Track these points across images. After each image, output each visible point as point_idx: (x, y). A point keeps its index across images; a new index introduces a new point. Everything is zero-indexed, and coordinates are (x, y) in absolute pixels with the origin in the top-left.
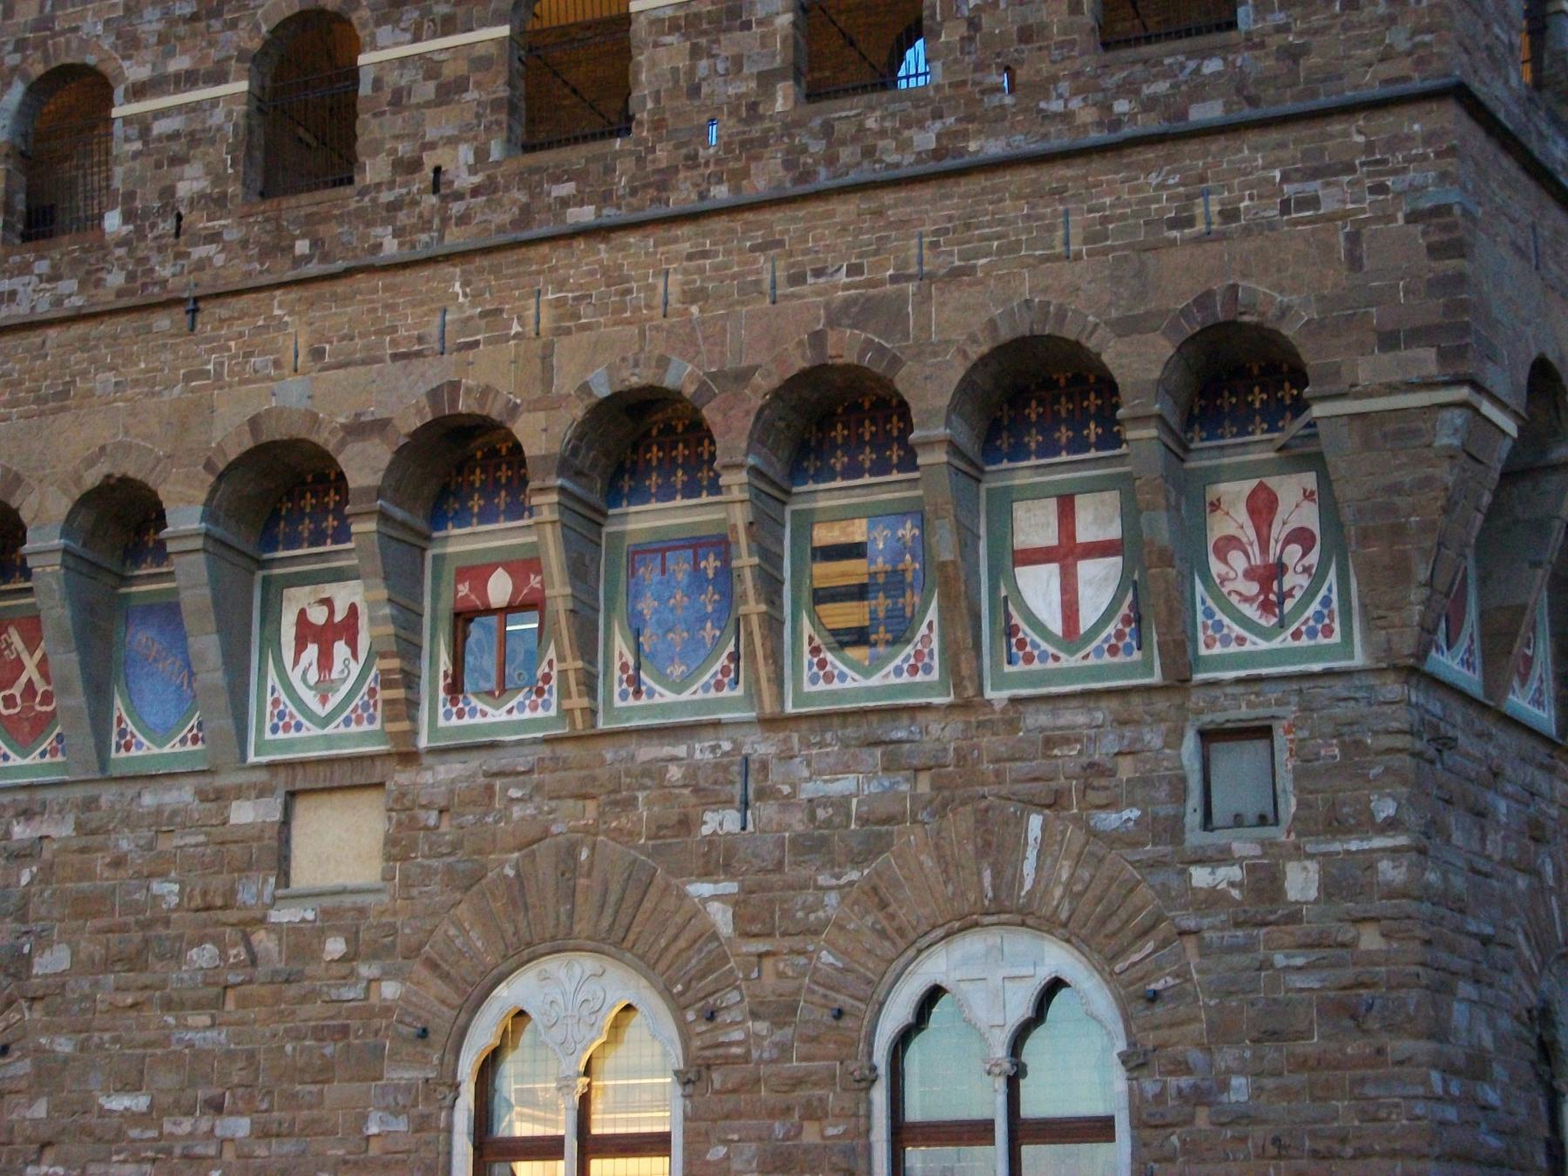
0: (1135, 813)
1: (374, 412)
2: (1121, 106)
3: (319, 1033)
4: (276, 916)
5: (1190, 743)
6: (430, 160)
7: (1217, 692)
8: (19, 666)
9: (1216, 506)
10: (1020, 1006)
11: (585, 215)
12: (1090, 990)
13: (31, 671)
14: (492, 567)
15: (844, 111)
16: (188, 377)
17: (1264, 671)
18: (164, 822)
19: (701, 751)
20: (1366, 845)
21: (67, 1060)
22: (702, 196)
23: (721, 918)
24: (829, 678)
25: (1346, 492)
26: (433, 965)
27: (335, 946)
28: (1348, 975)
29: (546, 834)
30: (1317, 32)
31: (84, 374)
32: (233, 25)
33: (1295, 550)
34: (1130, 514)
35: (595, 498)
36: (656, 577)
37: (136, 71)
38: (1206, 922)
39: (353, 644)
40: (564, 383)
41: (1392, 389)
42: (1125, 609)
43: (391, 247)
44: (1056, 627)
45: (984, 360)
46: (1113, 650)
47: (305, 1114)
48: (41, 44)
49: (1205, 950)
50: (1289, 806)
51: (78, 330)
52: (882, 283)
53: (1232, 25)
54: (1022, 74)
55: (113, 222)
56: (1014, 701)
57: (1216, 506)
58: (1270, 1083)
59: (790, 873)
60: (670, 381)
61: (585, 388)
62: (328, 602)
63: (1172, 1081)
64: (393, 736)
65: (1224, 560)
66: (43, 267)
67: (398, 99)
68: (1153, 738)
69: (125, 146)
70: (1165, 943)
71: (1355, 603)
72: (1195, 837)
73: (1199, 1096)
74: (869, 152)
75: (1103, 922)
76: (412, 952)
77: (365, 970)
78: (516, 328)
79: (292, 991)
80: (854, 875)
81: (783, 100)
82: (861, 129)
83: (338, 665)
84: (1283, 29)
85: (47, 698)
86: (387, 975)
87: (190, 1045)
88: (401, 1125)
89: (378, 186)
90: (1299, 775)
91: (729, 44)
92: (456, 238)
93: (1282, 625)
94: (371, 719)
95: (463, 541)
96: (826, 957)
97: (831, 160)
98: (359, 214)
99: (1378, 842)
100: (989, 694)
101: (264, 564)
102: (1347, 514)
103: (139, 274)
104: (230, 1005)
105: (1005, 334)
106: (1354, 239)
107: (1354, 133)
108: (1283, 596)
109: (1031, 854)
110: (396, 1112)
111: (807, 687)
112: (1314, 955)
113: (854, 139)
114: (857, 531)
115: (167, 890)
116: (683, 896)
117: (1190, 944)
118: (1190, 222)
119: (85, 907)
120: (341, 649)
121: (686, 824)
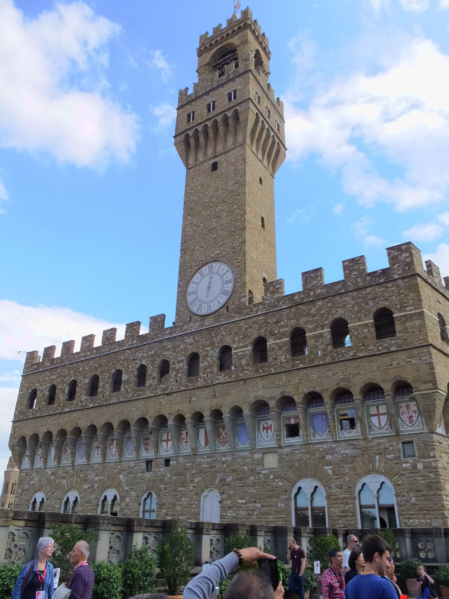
0: (393, 455)
1: (272, 396)
2: (380, 348)
3: (270, 491)
4: (262, 472)
5: (400, 445)
6: (278, 358)
7: (403, 436)
8: (222, 433)
9: (401, 407)
10: (379, 487)
11: (301, 366)
12: (389, 484)
13: (224, 434)
14: (291, 418)
15: (339, 349)
16: (245, 391)
17: (411, 433)
18: (245, 458)
19: (325, 446)
20: (429, 460)
21: (233, 495)
22: (319, 363)
23: (330, 472)
24: (344, 434)
25: (420, 405)
26: (286, 480)
27: (272, 477)
28: (429, 481)
29: (302, 459)
30: (409, 336)
31: (230, 391)
32: (248, 339)
33: (414, 414)
34: (387, 408)
35: (306, 408)
36: (316, 419)
37: (235, 346)
38: (406, 473)
39: (271, 430)
40: (300, 391)
41: (425, 390)
42: (388, 423)
43: (273, 371)
44: (378, 426)
45: (363, 386)
46: (387, 430)
47: (269, 503)
48: (221, 342)
49: (406, 477)
50: (417, 454)
51: (229, 384)
52: (346, 375)
53: (396, 336)
54: (365, 344)
55: (233, 368)
56: (373, 438)
57: (401, 407)
58: (418, 498)
59: (340, 465)
60: (316, 390)
61: (304, 391)
62: (267, 423)
63: (403, 498)
64: (278, 444)
65: (403, 415)
66: (223, 375)
67: (273, 349)
68: (395, 444)
69: (234, 357)
70: (399, 476)
71: (424, 422)
72: (403, 459)
73: (407, 501)
74: (343, 356)
75: (390, 473)
76: (283, 478)
77: (276, 480)
78: (293, 383)
79: (265, 484)
80: (350, 465)
81: (330, 348)
82: (342, 352)
83: (269, 433)
84: (403, 336)
85: (226, 438)
86: (280, 481)
87: (251, 492)
88: (283, 505)
89: (271, 362)
90: (418, 449)
91: (321, 340)
92: (283, 370)
93: (413, 426)
94: (275, 441)
95: (286, 414)
96: (347, 478)
97: (338, 357)
98: (268, 366)
99: (431, 460)
100: (369, 437)
101: (256, 418)
102: (421, 409)
103: (237, 376)
104: (256, 486)
105: (366, 383)
106: (417, 367)
107: (416, 351)
108: (413, 421)
109: (377, 462)
110: (282, 503)
111: (340, 436)
112: (423, 478)
113: (341, 354)
114: (346, 412)
115: (246, 468)
116: (324, 469)
117: (404, 476)
118: (392, 365)
119: (234, 471)
120: (269, 430)
121: (324, 458)
